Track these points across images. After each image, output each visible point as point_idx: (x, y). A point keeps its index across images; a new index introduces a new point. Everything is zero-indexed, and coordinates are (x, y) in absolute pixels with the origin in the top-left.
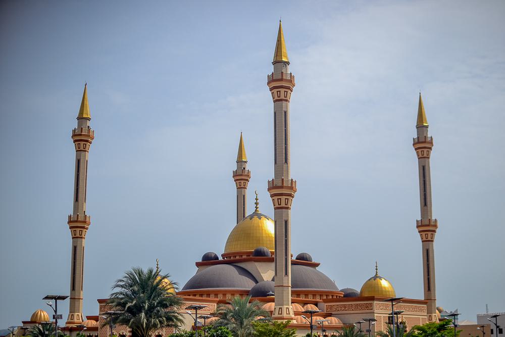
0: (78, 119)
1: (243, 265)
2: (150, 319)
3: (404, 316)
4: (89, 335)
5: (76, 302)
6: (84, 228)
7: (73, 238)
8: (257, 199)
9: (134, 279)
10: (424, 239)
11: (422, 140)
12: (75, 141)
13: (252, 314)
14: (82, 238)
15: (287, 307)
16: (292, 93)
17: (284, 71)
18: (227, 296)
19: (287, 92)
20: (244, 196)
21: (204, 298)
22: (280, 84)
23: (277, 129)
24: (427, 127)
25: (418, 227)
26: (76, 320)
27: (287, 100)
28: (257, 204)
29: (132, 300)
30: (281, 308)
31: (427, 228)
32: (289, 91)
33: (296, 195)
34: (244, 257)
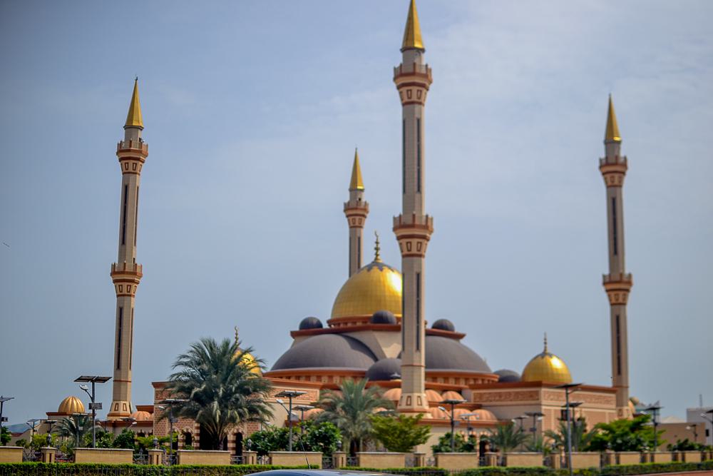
0: (126, 127)
1: (356, 335)
2: (226, 411)
3: (583, 410)
4: (139, 432)
5: (122, 387)
6: (133, 281)
7: (118, 296)
8: (377, 243)
9: (203, 355)
10: (614, 301)
11: (612, 160)
12: (121, 160)
13: (370, 404)
14: (130, 296)
15: (419, 394)
17: (416, 61)
18: (334, 378)
19: (421, 91)
20: (359, 239)
21: (302, 381)
22: (412, 80)
23: (407, 143)
24: (619, 143)
25: (605, 283)
26: (121, 411)
27: (420, 103)
28: (377, 249)
29: (201, 383)
30: (409, 397)
31: (617, 286)
32: (424, 91)
33: (432, 237)
34: (359, 324)
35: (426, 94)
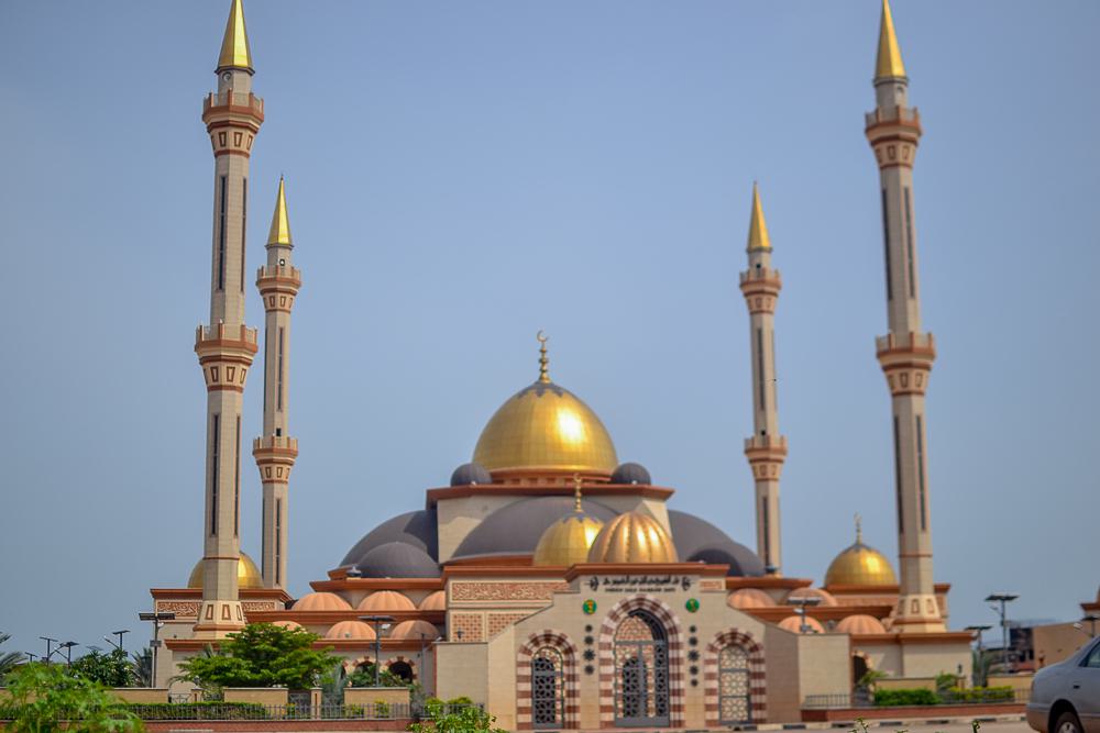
16: (918, 150)
26: (218, 621)
28: (543, 362)
30: (915, 601)
32: (912, 147)
35: (914, 151)
